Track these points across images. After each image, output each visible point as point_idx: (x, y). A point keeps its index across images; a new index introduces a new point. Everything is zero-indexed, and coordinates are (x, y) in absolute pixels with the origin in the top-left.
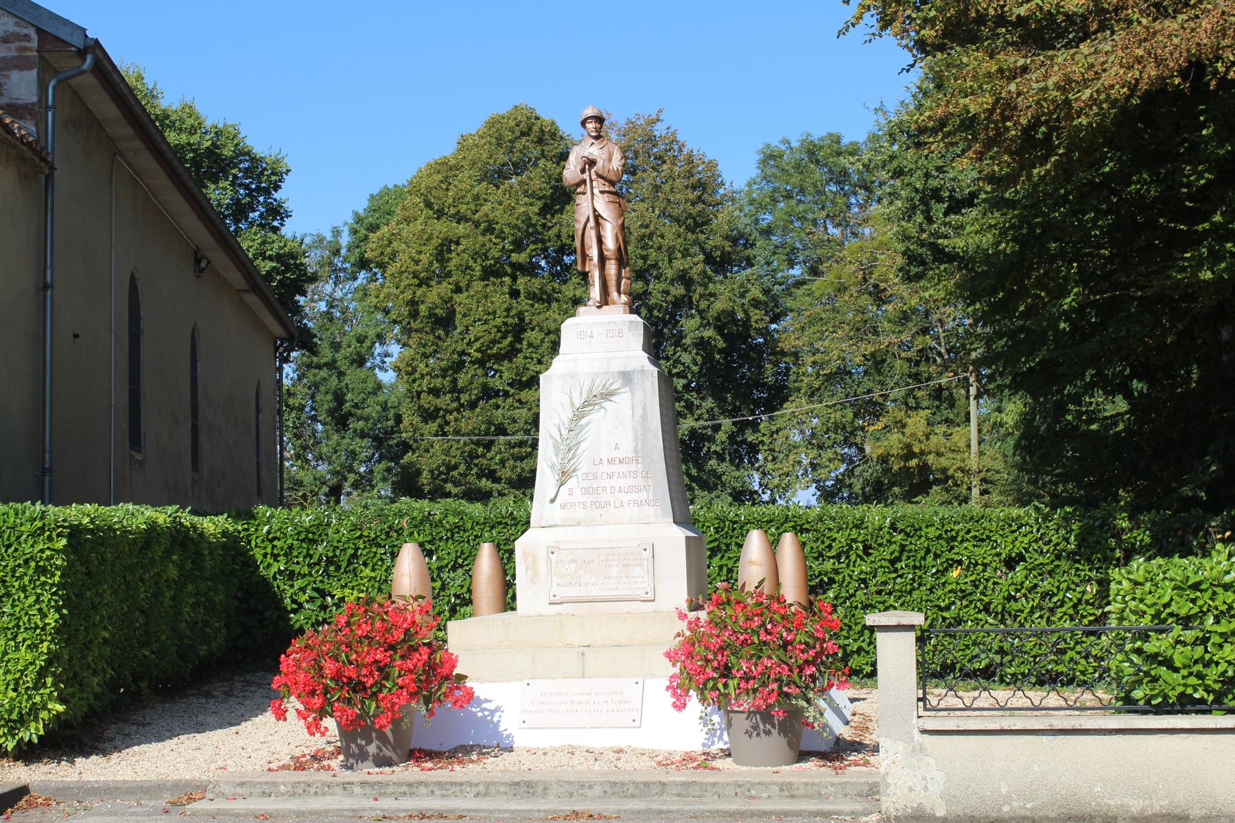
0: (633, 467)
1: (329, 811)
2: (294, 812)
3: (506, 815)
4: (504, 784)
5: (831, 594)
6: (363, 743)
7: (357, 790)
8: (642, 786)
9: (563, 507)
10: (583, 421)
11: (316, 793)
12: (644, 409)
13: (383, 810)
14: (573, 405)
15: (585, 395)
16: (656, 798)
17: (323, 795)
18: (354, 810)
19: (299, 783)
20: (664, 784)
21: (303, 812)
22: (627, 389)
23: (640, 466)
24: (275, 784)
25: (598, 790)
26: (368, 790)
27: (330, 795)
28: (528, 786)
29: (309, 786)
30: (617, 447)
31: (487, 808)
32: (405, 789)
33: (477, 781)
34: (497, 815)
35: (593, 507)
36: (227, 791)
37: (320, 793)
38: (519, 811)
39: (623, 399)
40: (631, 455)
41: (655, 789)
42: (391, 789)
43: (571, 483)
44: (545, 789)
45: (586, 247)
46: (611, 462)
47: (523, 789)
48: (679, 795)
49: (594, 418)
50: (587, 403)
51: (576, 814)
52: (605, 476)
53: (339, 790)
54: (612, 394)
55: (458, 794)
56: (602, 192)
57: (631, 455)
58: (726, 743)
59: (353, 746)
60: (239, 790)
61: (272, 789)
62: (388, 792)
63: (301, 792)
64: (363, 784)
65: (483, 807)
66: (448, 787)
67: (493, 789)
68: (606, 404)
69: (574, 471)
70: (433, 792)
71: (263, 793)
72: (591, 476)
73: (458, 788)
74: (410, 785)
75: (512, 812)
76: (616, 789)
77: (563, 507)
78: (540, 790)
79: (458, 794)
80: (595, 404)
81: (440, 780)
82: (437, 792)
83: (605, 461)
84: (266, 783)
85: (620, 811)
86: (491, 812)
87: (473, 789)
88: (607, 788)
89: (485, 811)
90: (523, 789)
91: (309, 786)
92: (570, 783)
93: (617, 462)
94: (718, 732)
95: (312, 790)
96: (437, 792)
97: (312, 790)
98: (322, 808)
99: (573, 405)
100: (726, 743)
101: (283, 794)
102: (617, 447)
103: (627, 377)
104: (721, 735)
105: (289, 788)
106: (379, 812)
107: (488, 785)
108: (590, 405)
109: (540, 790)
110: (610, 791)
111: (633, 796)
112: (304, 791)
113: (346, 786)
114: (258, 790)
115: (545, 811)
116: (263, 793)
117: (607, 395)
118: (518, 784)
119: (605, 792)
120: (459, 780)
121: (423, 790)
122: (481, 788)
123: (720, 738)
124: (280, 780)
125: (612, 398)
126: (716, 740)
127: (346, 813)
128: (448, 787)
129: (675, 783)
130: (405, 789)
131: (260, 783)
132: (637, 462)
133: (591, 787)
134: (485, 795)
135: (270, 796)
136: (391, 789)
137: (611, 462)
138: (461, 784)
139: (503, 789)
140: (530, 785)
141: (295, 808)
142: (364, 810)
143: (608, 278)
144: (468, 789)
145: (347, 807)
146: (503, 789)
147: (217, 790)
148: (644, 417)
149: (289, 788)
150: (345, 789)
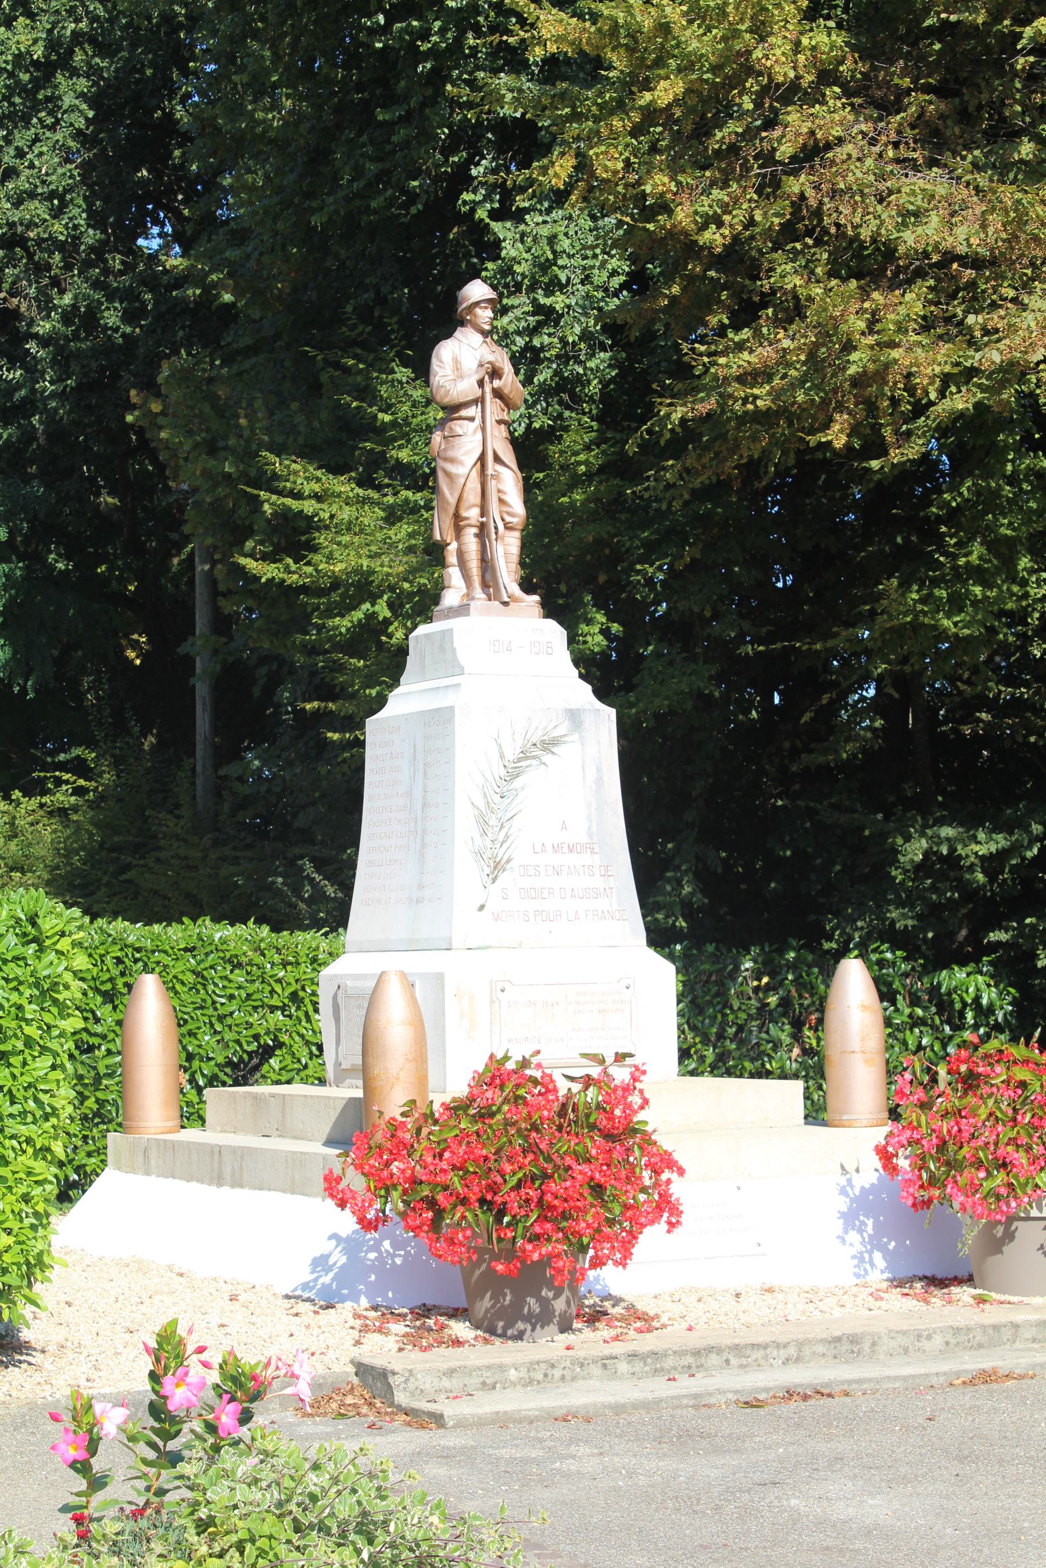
0: (587, 859)
1: (661, 1400)
2: (610, 1406)
3: (897, 1385)
4: (822, 1341)
5: (274, 1062)
6: (551, 1294)
7: (623, 1367)
8: (991, 1331)
9: (497, 918)
10: (517, 783)
11: (563, 1378)
12: (599, 770)
13: (736, 1392)
14: (502, 756)
15: (520, 743)
16: (1008, 1346)
17: (574, 1379)
18: (696, 1396)
19: (538, 1363)
20: (1016, 1326)
21: (624, 1406)
22: (575, 737)
23: (596, 856)
24: (502, 1368)
25: (938, 1341)
26: (638, 1366)
27: (584, 1378)
28: (852, 1342)
29: (553, 1366)
30: (564, 827)
31: (873, 1375)
32: (689, 1360)
33: (785, 1340)
34: (886, 1385)
35: (539, 918)
36: (428, 1386)
37: (568, 1378)
38: (914, 1377)
39: (568, 752)
40: (584, 839)
41: (1006, 1334)
42: (670, 1362)
43: (504, 878)
44: (874, 1344)
45: (464, 505)
46: (557, 848)
47: (845, 1347)
48: (1034, 1340)
49: (533, 777)
50: (525, 756)
51: (986, 1377)
52: (550, 871)
53: (596, 1370)
54: (555, 742)
55: (762, 1362)
56: (499, 422)
57: (584, 839)
58: (882, 1272)
59: (531, 1301)
60: (446, 1383)
61: (497, 1377)
62: (666, 1366)
63: (540, 1377)
64: (633, 1356)
65: (867, 1375)
66: (748, 1352)
67: (807, 1351)
68: (547, 758)
69: (508, 861)
70: (727, 1361)
71: (484, 1384)
72: (531, 871)
73: (760, 1354)
74: (697, 1353)
75: (905, 1378)
76: (962, 1338)
77: (497, 918)
78: (866, 1347)
79: (762, 1362)
80: (534, 757)
81: (737, 1341)
82: (734, 1361)
83: (549, 848)
84: (488, 1368)
85: (1034, 1366)
86: (878, 1381)
87: (782, 1352)
88: (949, 1337)
89: (870, 1380)
90: (845, 1347)
91: (553, 1366)
92: (904, 1333)
93: (566, 849)
94: (866, 1256)
95: (557, 1373)
96: (734, 1361)
97: (557, 1373)
98: (650, 1397)
99: (502, 756)
100: (882, 1272)
101: (514, 1384)
102: (564, 827)
103: (574, 716)
104: (871, 1258)
105: (523, 1373)
106: (730, 1396)
107: (800, 1344)
108: (527, 758)
109: (866, 1347)
110: (953, 1341)
111: (980, 1346)
112: (546, 1375)
113: (606, 1362)
114: (475, 1381)
115: (945, 1374)
116: (484, 1384)
117: (549, 745)
118: (838, 1340)
119: (947, 1343)
120: (760, 1340)
121: (714, 1359)
122: (792, 1351)
123: (872, 1264)
124: (507, 1360)
125: (555, 750)
126: (868, 1266)
127: (685, 1401)
128: (748, 1352)
129: (1030, 1324)
130: (689, 1360)
131: (479, 1369)
132: (593, 852)
133: (929, 1337)
134: (798, 1360)
135: (494, 1388)
136: (670, 1362)
137: (557, 848)
138: (766, 1347)
139: (820, 1349)
140: (854, 1339)
141: (611, 1399)
142: (711, 1395)
143: (467, 557)
144: (775, 1353)
145: (684, 1392)
146: (820, 1349)
147: (411, 1386)
148: (599, 781)
149: (523, 1373)
150: (605, 1366)
